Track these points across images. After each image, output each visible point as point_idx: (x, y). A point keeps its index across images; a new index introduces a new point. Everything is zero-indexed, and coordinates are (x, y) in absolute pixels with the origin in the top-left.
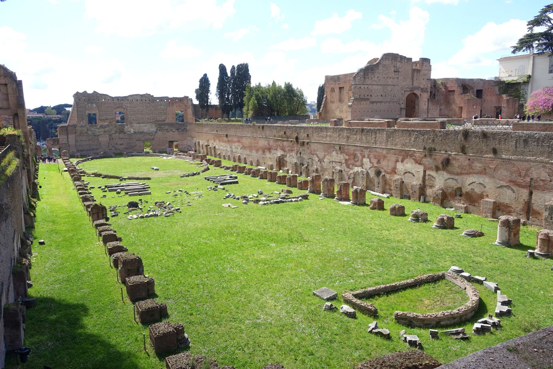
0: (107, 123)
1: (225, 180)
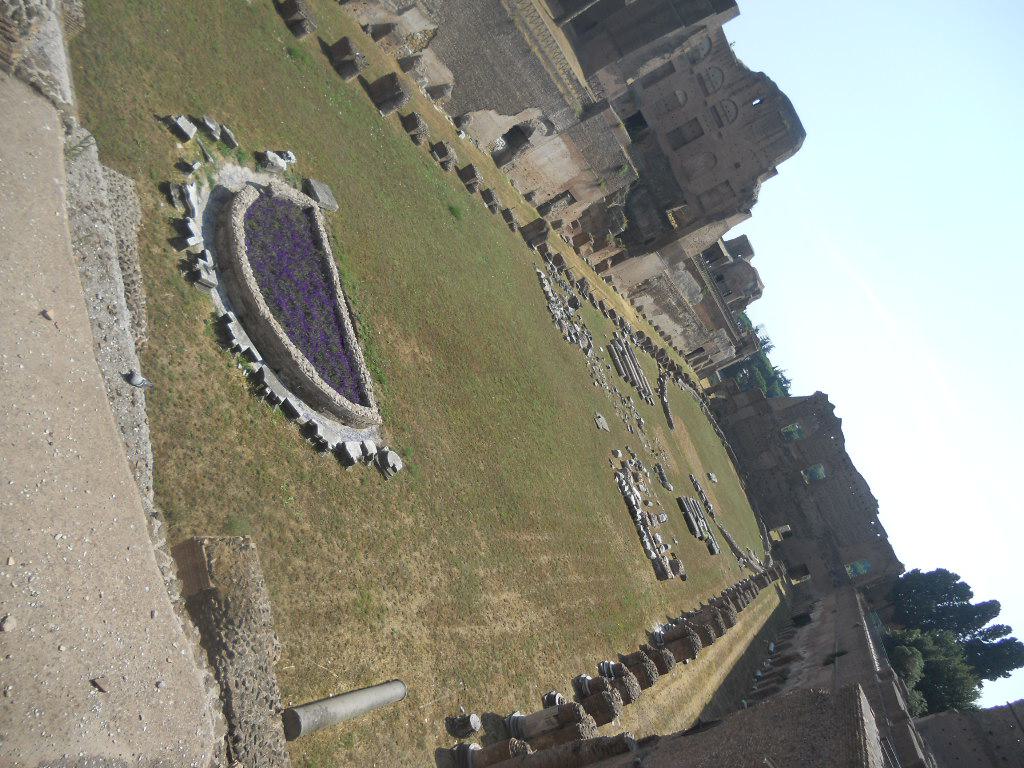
0: (795, 456)
1: (697, 520)
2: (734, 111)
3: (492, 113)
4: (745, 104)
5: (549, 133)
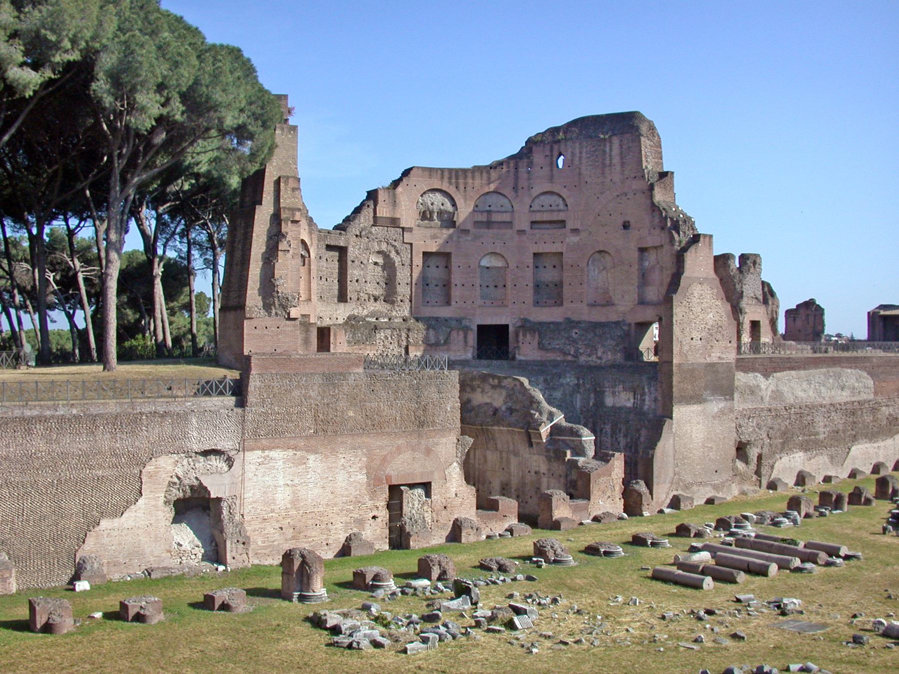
2: (555, 198)
3: (105, 523)
4: (551, 178)
5: (230, 462)
